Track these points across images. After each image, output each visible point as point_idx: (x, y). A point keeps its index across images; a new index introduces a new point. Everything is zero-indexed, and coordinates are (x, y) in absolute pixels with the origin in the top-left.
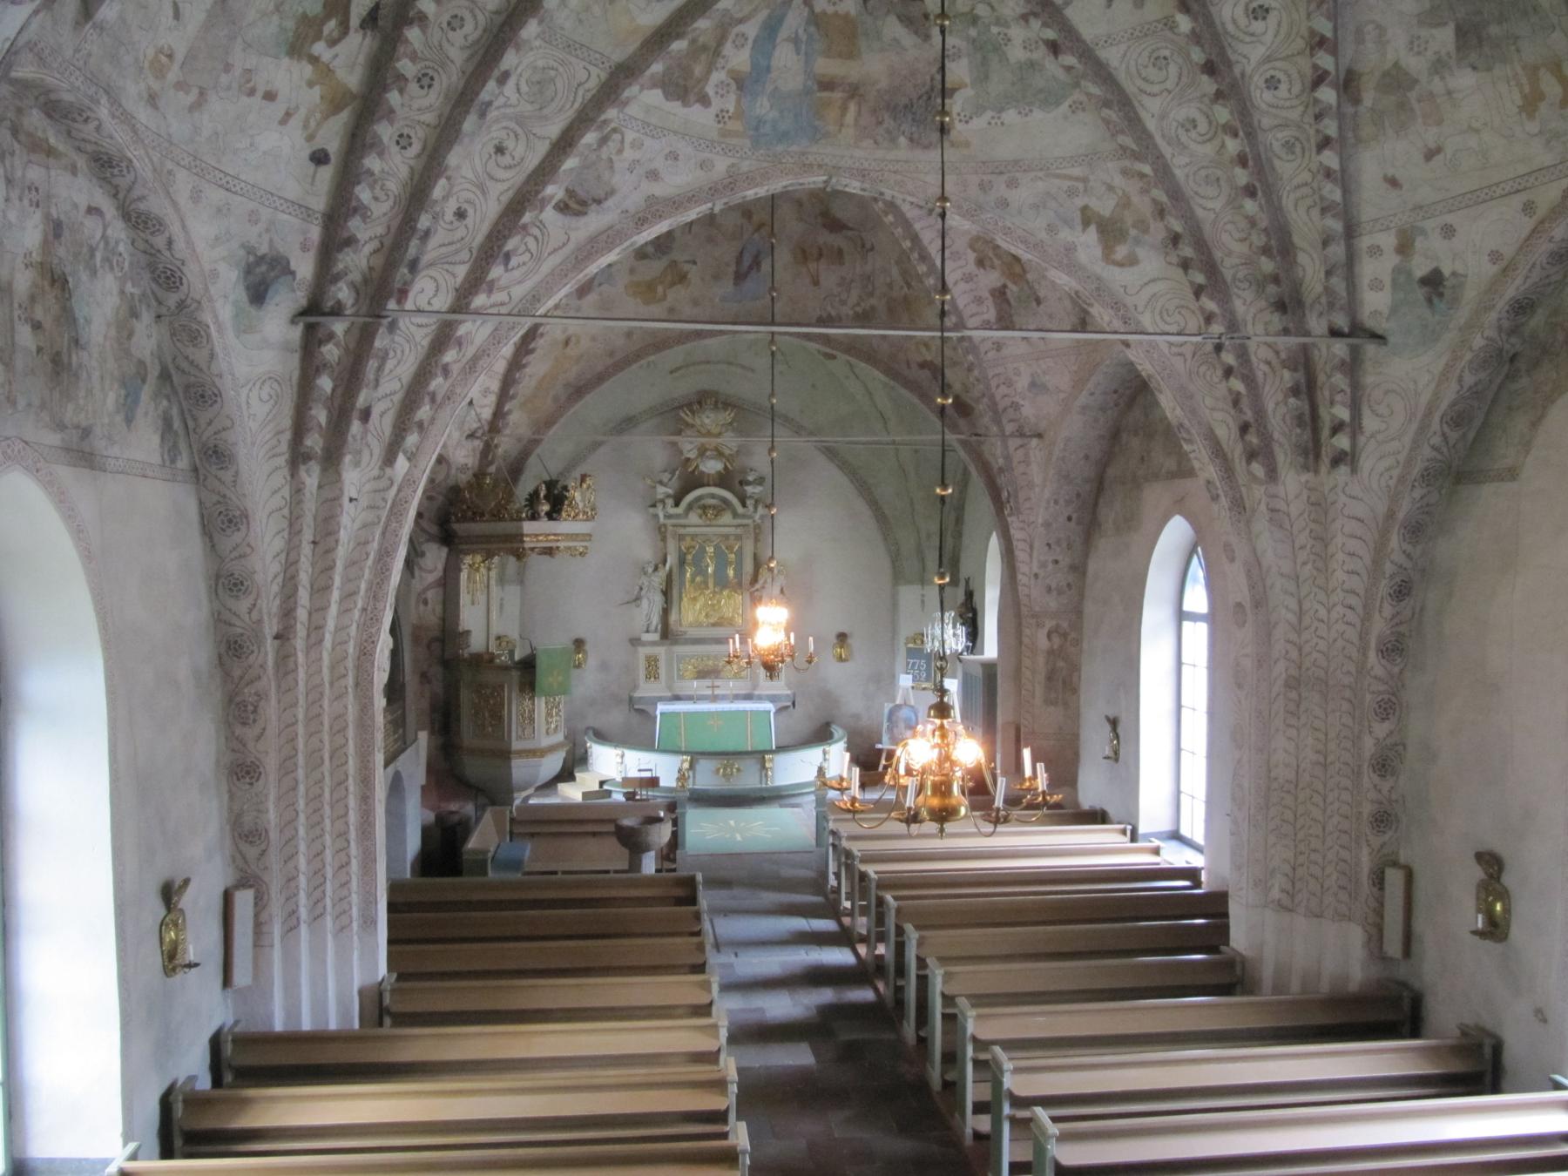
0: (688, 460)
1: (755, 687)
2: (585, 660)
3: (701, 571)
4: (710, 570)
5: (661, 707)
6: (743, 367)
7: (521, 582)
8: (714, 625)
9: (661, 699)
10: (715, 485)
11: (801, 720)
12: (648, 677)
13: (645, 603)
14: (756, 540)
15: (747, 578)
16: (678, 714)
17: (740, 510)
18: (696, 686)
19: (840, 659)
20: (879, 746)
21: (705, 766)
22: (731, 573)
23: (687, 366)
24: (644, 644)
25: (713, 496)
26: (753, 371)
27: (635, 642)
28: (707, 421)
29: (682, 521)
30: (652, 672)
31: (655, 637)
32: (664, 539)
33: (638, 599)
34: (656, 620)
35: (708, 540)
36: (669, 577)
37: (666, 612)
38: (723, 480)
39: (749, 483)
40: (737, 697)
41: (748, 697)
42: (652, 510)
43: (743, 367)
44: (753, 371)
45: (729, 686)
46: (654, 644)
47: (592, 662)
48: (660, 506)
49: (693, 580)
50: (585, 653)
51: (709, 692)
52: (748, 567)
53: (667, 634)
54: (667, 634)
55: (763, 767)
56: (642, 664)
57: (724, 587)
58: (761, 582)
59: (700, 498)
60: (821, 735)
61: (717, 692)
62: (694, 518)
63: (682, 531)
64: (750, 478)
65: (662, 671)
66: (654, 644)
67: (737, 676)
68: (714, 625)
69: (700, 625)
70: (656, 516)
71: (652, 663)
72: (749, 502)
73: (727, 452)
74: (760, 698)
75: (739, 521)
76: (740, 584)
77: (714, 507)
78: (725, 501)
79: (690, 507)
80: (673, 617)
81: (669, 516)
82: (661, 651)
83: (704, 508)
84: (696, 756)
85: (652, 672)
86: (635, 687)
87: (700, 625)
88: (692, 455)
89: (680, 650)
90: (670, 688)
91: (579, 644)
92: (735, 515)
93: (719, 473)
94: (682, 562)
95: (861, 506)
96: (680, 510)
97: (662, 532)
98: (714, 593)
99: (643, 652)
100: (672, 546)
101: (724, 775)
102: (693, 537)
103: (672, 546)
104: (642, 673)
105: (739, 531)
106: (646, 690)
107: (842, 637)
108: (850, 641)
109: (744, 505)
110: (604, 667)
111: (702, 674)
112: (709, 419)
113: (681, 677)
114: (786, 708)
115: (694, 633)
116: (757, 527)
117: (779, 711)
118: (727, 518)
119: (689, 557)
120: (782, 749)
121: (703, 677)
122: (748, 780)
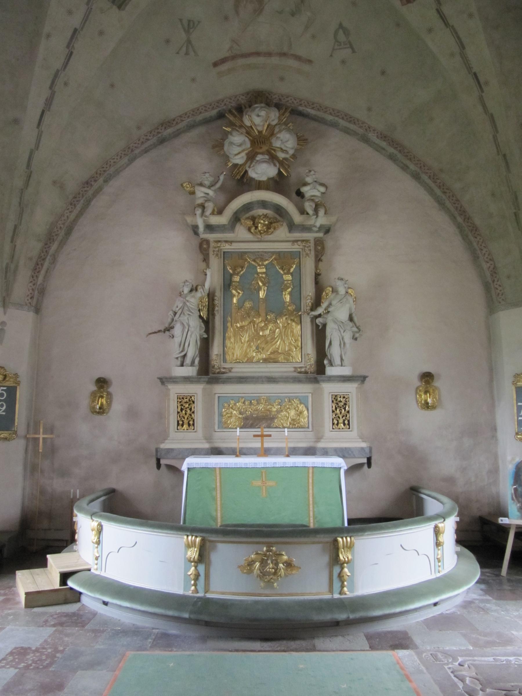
0: (235, 165)
1: (318, 439)
2: (109, 404)
3: (251, 292)
4: (262, 294)
5: (190, 462)
6: (298, 58)
7: (37, 310)
8: (266, 361)
9: (195, 452)
10: (267, 188)
11: (378, 487)
12: (180, 424)
13: (177, 330)
14: (318, 260)
15: (307, 301)
16: (211, 470)
17: (297, 218)
18: (240, 437)
19: (426, 406)
20: (503, 521)
21: (228, 556)
22: (288, 298)
23: (234, 57)
24: (174, 380)
25: (264, 204)
26: (310, 62)
27: (164, 381)
28: (257, 121)
29: (229, 236)
30: (186, 418)
31: (190, 371)
32: (206, 260)
33: (169, 329)
34: (192, 351)
35: (260, 256)
36: (211, 296)
37: (205, 345)
38: (278, 184)
39: (305, 184)
40: (293, 452)
41: (310, 451)
42: (189, 220)
43: (298, 58)
44: (310, 62)
45: (281, 437)
46: (187, 380)
47: (118, 406)
48: (199, 212)
49: (240, 305)
50: (109, 395)
51: (258, 445)
52: (309, 290)
53: (207, 371)
54: (207, 371)
55: (335, 560)
56: (173, 406)
57: (280, 314)
58: (324, 305)
59: (248, 207)
60: (404, 508)
61: (267, 445)
62: (241, 232)
63: (227, 247)
64: (309, 180)
65: (199, 417)
66: (187, 380)
67: (295, 425)
68: (266, 361)
69: (250, 361)
70: (195, 229)
71: (186, 404)
72: (309, 207)
73: (281, 155)
74: (325, 453)
75: (297, 235)
76: (298, 309)
77: (266, 216)
78: (279, 210)
79: (236, 218)
80: (216, 350)
81: (210, 228)
82: (197, 390)
83: (253, 219)
84: (209, 537)
85: (186, 418)
86: (165, 436)
87: (250, 361)
88: (239, 160)
89: (221, 389)
90: (208, 438)
91: (102, 383)
92: (292, 227)
93: (272, 179)
94: (227, 285)
95: (441, 219)
96: (223, 220)
97: (203, 249)
98: (267, 321)
99: (176, 390)
100: (215, 262)
101: (263, 574)
102: (242, 255)
103: (215, 262)
104: (173, 419)
105: (296, 248)
106: (177, 440)
107: (427, 377)
108: (436, 383)
109: (303, 212)
110: (132, 413)
111: (249, 422)
112: (259, 118)
113: (223, 425)
114: (361, 465)
115: (240, 370)
116: (320, 245)
117: (353, 469)
118: (282, 232)
119: (236, 279)
120: (361, 524)
121: (252, 426)
122: (306, 584)
